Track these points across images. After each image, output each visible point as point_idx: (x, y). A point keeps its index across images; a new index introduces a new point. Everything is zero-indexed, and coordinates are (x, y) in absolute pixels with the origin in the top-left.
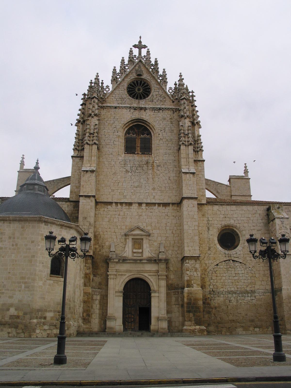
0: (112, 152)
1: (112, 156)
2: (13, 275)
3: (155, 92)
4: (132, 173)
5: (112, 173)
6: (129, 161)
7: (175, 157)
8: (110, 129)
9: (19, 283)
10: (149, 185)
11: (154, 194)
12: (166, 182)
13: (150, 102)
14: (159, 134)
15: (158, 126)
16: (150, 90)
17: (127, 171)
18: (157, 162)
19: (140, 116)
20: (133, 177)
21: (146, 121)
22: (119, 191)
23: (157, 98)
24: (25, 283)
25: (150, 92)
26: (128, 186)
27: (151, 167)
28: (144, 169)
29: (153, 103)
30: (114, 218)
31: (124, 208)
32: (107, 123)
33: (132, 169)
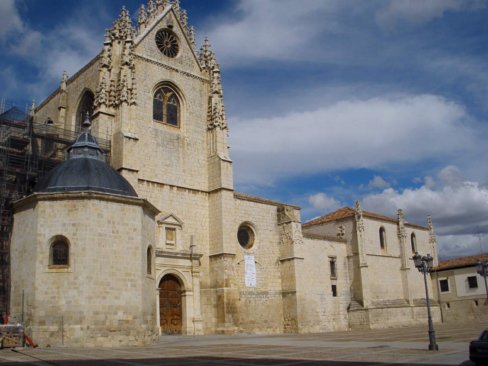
2: (117, 270)
8: (141, 86)
9: (125, 280)
11: (184, 177)
17: (158, 145)
21: (177, 87)
24: (132, 280)
31: (156, 189)
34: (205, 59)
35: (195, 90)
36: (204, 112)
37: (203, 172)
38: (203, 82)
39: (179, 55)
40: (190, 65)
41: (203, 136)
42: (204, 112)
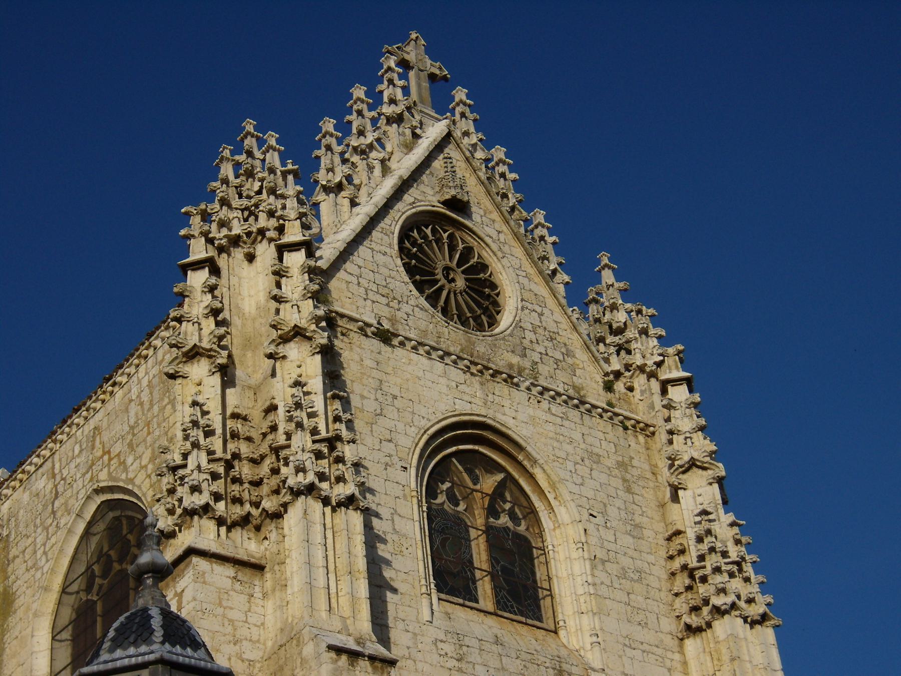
3: (527, 311)
7: (669, 670)
15: (575, 489)
21: (520, 448)
34: (616, 339)
35: (598, 462)
36: (651, 558)
38: (626, 428)
39: (505, 320)
40: (557, 361)
41: (668, 663)
42: (651, 558)
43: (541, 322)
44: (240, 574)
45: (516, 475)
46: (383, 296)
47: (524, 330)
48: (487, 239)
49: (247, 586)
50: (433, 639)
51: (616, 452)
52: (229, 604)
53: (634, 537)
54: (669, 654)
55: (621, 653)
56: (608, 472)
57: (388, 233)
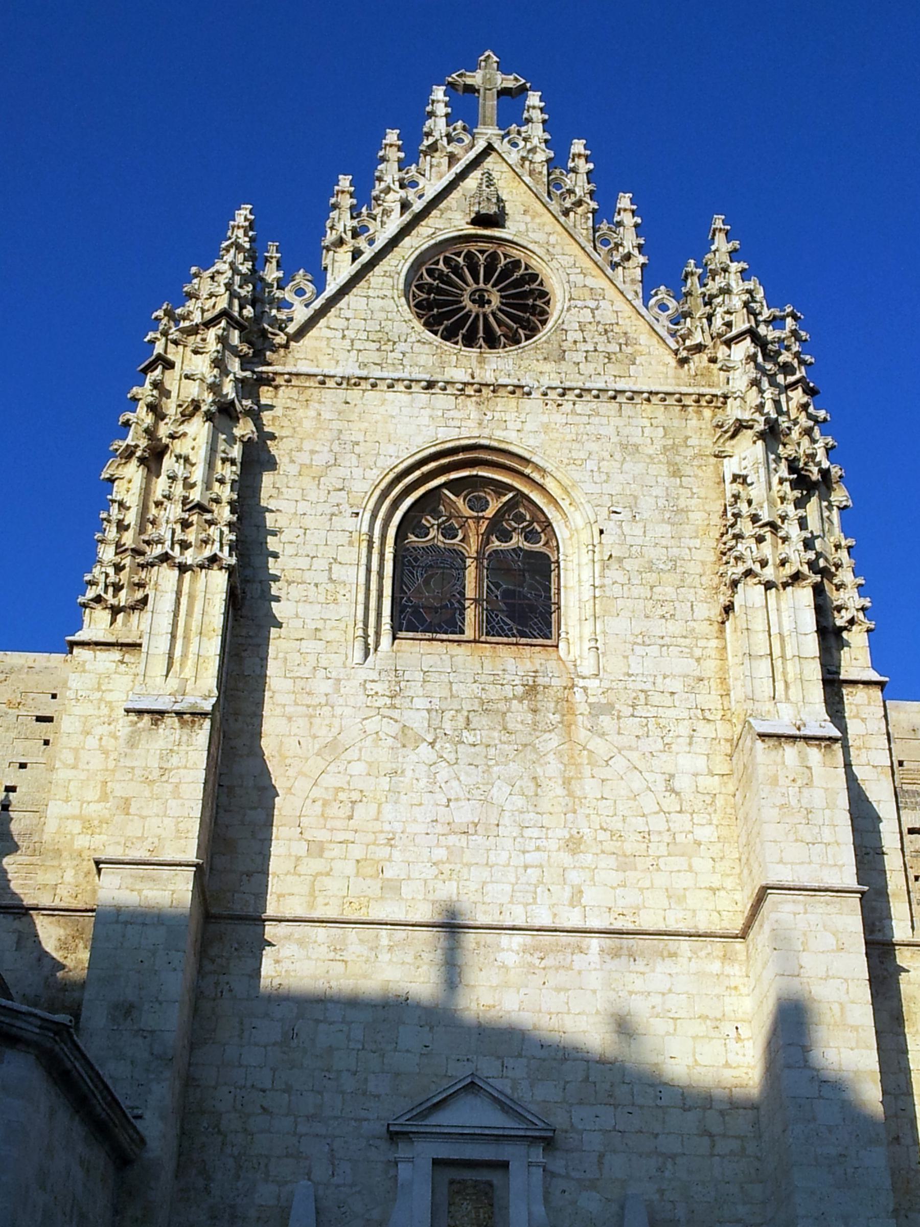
0: (320, 624)
1: (320, 646)
3: (573, 311)
4: (437, 746)
5: (317, 746)
6: (419, 676)
7: (698, 660)
8: (312, 496)
10: (546, 820)
12: (648, 803)
13: (545, 359)
14: (601, 532)
15: (596, 489)
16: (548, 303)
18: (592, 684)
19: (486, 432)
20: (444, 772)
21: (526, 461)
22: (357, 852)
23: (585, 341)
25: (543, 315)
26: (415, 820)
27: (557, 717)
28: (511, 726)
29: (564, 366)
30: (318, 1021)
32: (292, 461)
33: (436, 723)
36: (697, 544)
37: (705, 833)
41: (698, 652)
43: (594, 317)
44: (127, 656)
45: (526, 490)
46: (374, 341)
47: (566, 331)
48: (530, 246)
49: (133, 666)
50: (362, 681)
51: (665, 435)
52: (110, 687)
53: (673, 524)
54: (702, 643)
55: (629, 652)
56: (648, 460)
57: (392, 274)
